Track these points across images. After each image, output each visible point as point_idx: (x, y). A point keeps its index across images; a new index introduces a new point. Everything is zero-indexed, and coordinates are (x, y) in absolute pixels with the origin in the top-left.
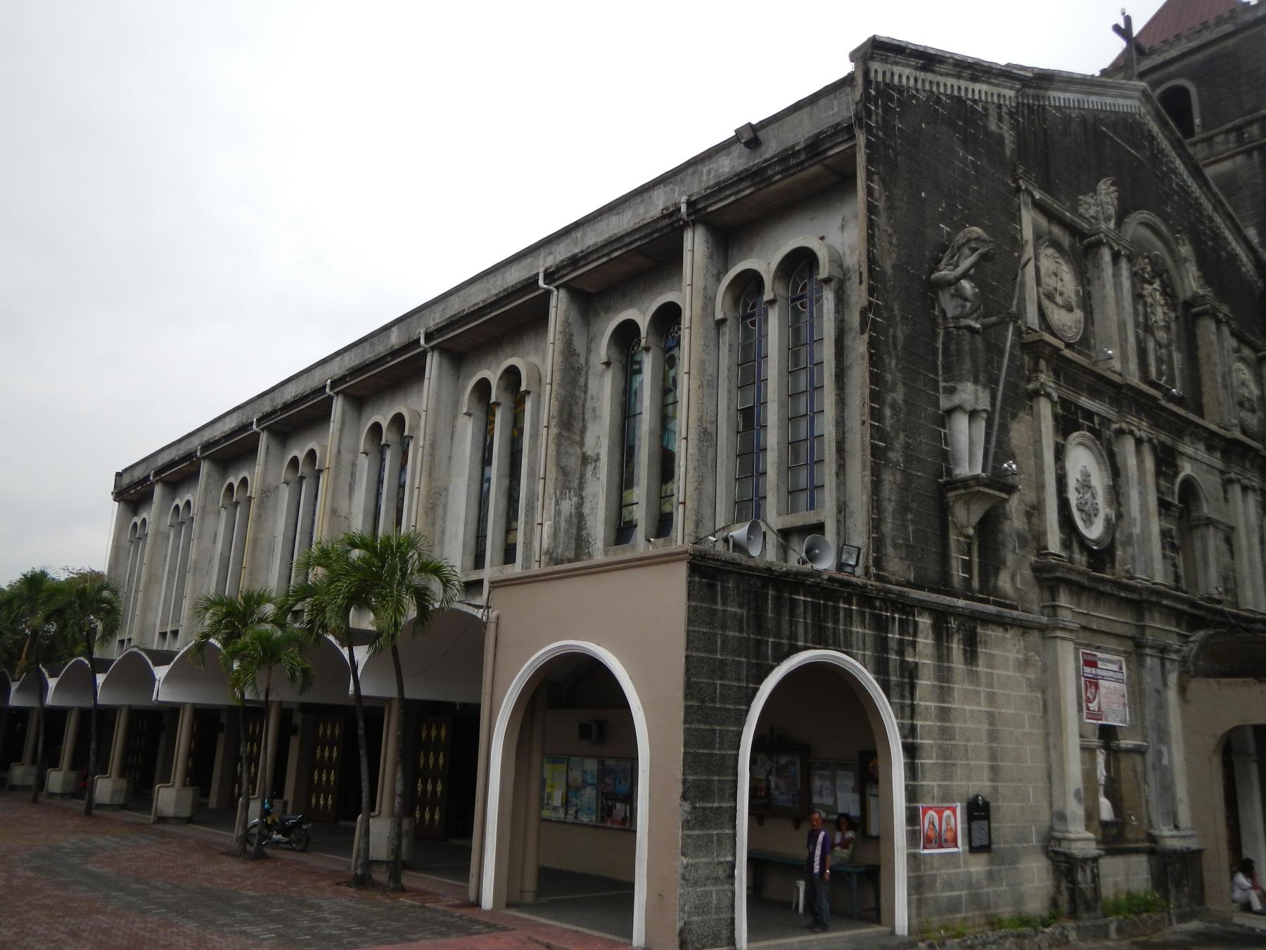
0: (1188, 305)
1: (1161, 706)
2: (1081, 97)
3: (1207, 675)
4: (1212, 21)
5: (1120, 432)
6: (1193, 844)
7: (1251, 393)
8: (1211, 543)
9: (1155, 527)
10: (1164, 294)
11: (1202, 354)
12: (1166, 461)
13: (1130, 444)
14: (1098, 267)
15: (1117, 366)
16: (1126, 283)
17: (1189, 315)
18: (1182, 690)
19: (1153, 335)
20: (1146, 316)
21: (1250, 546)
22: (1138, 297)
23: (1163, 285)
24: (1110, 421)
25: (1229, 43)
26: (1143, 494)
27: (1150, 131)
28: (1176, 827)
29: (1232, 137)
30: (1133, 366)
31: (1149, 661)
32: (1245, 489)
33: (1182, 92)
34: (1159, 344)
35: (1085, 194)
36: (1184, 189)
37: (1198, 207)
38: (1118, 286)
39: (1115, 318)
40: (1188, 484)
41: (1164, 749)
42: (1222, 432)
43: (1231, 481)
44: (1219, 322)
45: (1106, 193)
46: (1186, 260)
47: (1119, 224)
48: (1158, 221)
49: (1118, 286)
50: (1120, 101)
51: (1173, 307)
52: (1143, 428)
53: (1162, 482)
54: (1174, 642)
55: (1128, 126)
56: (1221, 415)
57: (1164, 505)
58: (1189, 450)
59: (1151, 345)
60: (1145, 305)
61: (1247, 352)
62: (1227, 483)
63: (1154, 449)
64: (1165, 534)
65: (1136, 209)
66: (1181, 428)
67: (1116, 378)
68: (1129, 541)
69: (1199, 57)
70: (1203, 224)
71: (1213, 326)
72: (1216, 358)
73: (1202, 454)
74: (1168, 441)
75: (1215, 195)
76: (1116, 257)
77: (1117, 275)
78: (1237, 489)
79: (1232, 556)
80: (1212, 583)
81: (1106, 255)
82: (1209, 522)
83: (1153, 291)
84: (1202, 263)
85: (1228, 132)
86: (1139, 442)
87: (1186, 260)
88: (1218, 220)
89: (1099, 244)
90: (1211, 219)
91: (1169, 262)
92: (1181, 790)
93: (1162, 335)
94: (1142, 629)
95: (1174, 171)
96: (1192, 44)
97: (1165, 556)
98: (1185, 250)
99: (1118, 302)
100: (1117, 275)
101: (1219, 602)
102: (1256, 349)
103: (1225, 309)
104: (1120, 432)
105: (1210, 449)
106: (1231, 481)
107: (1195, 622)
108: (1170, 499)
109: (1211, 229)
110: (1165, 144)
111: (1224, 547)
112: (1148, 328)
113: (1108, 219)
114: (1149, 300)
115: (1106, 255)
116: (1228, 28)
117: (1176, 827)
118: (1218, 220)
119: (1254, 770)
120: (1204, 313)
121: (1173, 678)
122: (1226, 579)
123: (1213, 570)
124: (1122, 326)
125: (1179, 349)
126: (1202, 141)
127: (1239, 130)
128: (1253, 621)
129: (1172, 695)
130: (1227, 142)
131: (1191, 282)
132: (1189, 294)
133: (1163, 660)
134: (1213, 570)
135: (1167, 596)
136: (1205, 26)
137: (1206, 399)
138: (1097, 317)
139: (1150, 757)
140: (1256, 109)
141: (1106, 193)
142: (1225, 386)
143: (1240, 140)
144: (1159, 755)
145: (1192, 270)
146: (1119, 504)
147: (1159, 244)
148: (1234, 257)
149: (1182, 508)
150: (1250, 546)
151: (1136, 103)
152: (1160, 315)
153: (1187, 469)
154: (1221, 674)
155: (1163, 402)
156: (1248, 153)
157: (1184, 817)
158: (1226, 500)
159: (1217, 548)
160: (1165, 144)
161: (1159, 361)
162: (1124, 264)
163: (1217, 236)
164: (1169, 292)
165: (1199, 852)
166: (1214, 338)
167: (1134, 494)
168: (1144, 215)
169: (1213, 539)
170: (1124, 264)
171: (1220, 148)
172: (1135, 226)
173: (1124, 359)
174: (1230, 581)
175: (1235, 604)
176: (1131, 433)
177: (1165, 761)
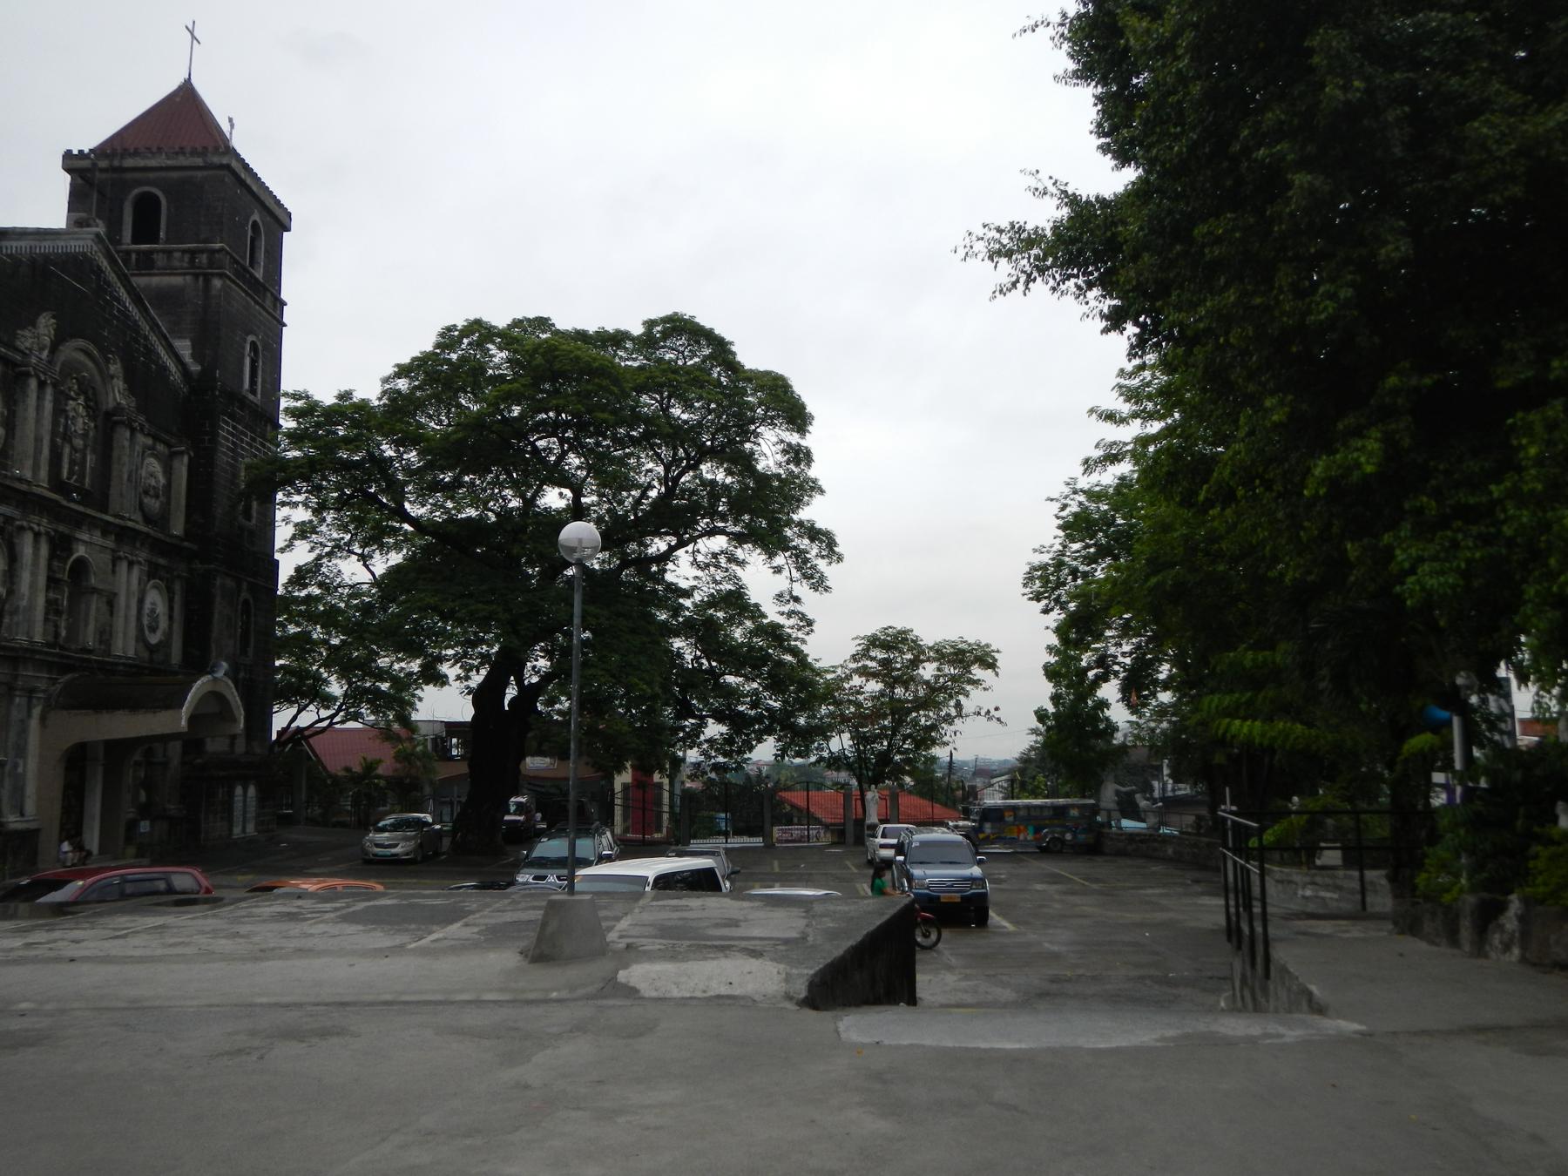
0: (108, 414)
1: (23, 731)
2: (33, 243)
3: (64, 708)
4: (188, 150)
5: (21, 528)
6: (33, 826)
7: (157, 481)
8: (94, 607)
9: (41, 600)
10: (87, 407)
11: (115, 454)
12: (60, 546)
13: (28, 538)
14: (25, 394)
15: (28, 475)
16: (48, 405)
17: (107, 423)
18: (43, 719)
19: (70, 442)
20: (66, 426)
21: (128, 607)
22: (59, 411)
23: (87, 400)
24: (13, 519)
25: (199, 174)
26: (34, 574)
27: (99, 267)
28: (22, 815)
29: (187, 257)
30: (43, 473)
31: (17, 700)
32: (131, 564)
33: (155, 201)
34: (74, 449)
35: (23, 328)
36: (125, 314)
37: (136, 327)
38: (39, 408)
39: (32, 436)
40: (81, 562)
41: (21, 762)
42: (117, 521)
43: (120, 558)
44: (133, 430)
45: (46, 325)
46: (112, 377)
47: (54, 349)
48: (91, 347)
49: (39, 408)
50: (72, 243)
51: (93, 418)
52: (44, 524)
53: (55, 563)
54: (42, 685)
55: (78, 264)
56: (124, 507)
57: (53, 582)
58: (85, 537)
59: (67, 450)
60: (67, 418)
61: (160, 447)
62: (115, 560)
63: (51, 541)
64: (49, 602)
65: (73, 336)
66: (79, 521)
67: (24, 487)
68: (15, 612)
69: (175, 175)
70: (137, 342)
71: (128, 434)
72: (126, 459)
73: (97, 538)
74: (66, 531)
75: (153, 319)
76: (42, 385)
77: (40, 398)
78: (124, 566)
79: (112, 614)
80: (90, 638)
81: (33, 383)
82: (94, 590)
83: (77, 406)
84: (130, 376)
85: (184, 251)
86: (37, 535)
87: (112, 377)
88: (153, 338)
89: (28, 375)
90: (146, 338)
91: (98, 378)
92: (30, 789)
93: (79, 442)
94: (16, 677)
95: (118, 300)
96: (170, 163)
97: (46, 620)
98: (115, 368)
99: (38, 421)
100: (40, 398)
101: (90, 652)
102: (169, 446)
103: (142, 419)
104: (21, 528)
105: (105, 534)
106: (120, 558)
107: (65, 669)
108: (59, 576)
109: (146, 347)
110: (112, 277)
111: (104, 608)
112: (67, 437)
113: (41, 349)
114: (71, 414)
115: (33, 383)
116: (199, 161)
117: (22, 815)
118: (153, 338)
119: (100, 769)
120: (122, 422)
121: (37, 711)
122: (102, 633)
123: (91, 627)
124: (38, 440)
125: (94, 451)
126: (163, 251)
127: (193, 253)
128: (117, 664)
129: (34, 723)
130: (181, 260)
131: (117, 394)
132: (111, 405)
133: (30, 698)
134: (91, 627)
135: (40, 652)
136: (182, 151)
137: (114, 492)
138: (18, 433)
139: (8, 768)
140: (206, 241)
141: (46, 325)
142: (129, 480)
143: (192, 261)
144: (16, 766)
145: (119, 384)
146: (12, 583)
147: (90, 364)
148: (165, 368)
149: (71, 580)
150: (128, 607)
151: (90, 243)
152: (80, 422)
153: (81, 551)
154: (74, 708)
155: (65, 503)
156: (196, 276)
157: (30, 807)
158: (114, 572)
159: (98, 609)
160: (112, 277)
161: (72, 462)
162: (49, 391)
163: (150, 352)
164: (93, 408)
165: (37, 831)
166: (127, 444)
167: (25, 577)
168: (81, 343)
169: (95, 605)
170: (49, 391)
171: (176, 264)
172: (71, 351)
173: (36, 468)
174: (105, 635)
175: (108, 653)
176: (31, 529)
177: (20, 770)
